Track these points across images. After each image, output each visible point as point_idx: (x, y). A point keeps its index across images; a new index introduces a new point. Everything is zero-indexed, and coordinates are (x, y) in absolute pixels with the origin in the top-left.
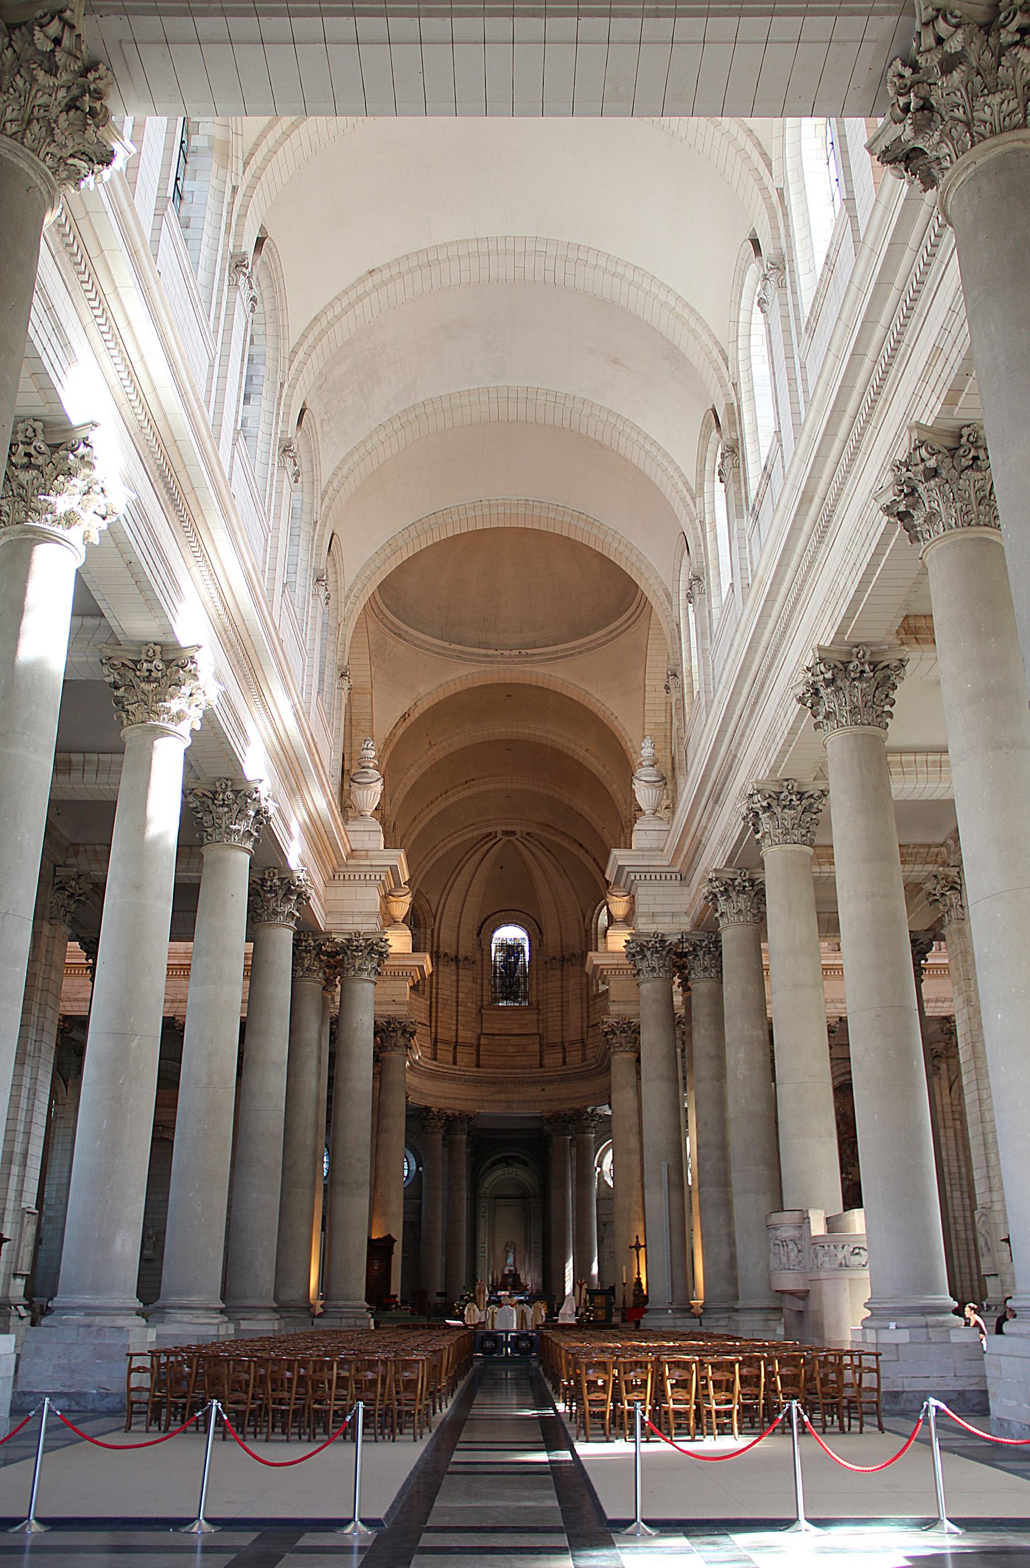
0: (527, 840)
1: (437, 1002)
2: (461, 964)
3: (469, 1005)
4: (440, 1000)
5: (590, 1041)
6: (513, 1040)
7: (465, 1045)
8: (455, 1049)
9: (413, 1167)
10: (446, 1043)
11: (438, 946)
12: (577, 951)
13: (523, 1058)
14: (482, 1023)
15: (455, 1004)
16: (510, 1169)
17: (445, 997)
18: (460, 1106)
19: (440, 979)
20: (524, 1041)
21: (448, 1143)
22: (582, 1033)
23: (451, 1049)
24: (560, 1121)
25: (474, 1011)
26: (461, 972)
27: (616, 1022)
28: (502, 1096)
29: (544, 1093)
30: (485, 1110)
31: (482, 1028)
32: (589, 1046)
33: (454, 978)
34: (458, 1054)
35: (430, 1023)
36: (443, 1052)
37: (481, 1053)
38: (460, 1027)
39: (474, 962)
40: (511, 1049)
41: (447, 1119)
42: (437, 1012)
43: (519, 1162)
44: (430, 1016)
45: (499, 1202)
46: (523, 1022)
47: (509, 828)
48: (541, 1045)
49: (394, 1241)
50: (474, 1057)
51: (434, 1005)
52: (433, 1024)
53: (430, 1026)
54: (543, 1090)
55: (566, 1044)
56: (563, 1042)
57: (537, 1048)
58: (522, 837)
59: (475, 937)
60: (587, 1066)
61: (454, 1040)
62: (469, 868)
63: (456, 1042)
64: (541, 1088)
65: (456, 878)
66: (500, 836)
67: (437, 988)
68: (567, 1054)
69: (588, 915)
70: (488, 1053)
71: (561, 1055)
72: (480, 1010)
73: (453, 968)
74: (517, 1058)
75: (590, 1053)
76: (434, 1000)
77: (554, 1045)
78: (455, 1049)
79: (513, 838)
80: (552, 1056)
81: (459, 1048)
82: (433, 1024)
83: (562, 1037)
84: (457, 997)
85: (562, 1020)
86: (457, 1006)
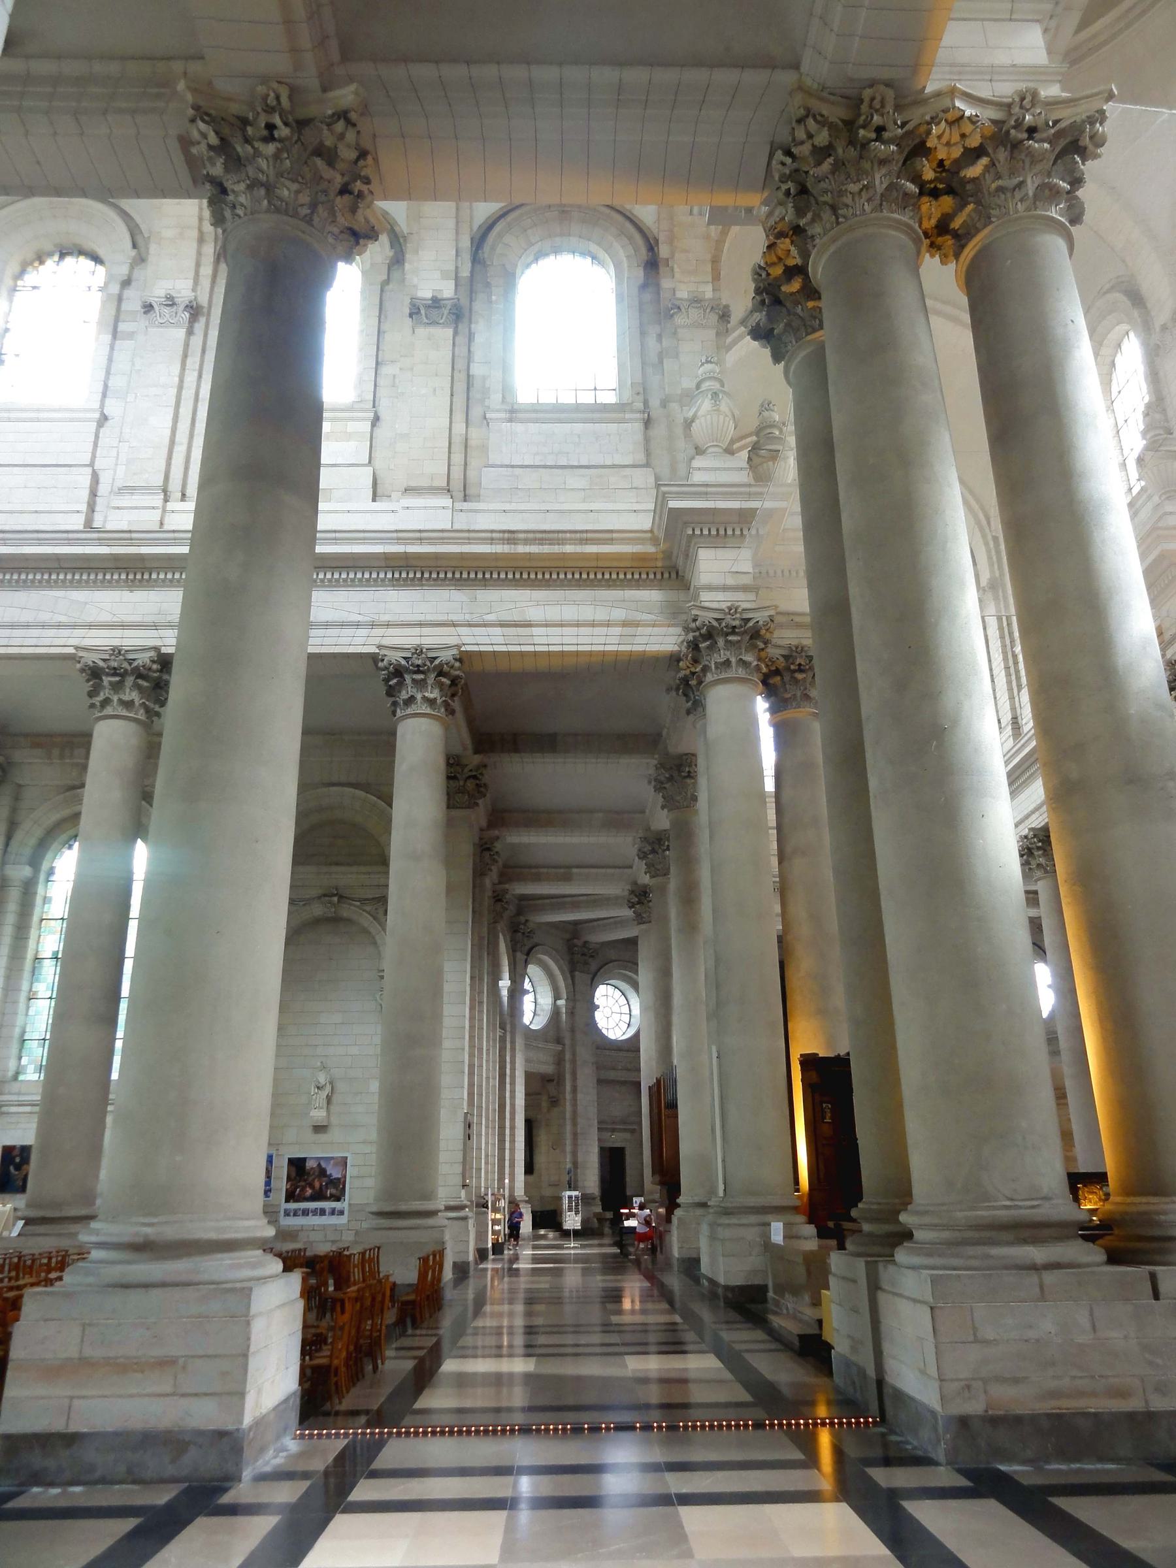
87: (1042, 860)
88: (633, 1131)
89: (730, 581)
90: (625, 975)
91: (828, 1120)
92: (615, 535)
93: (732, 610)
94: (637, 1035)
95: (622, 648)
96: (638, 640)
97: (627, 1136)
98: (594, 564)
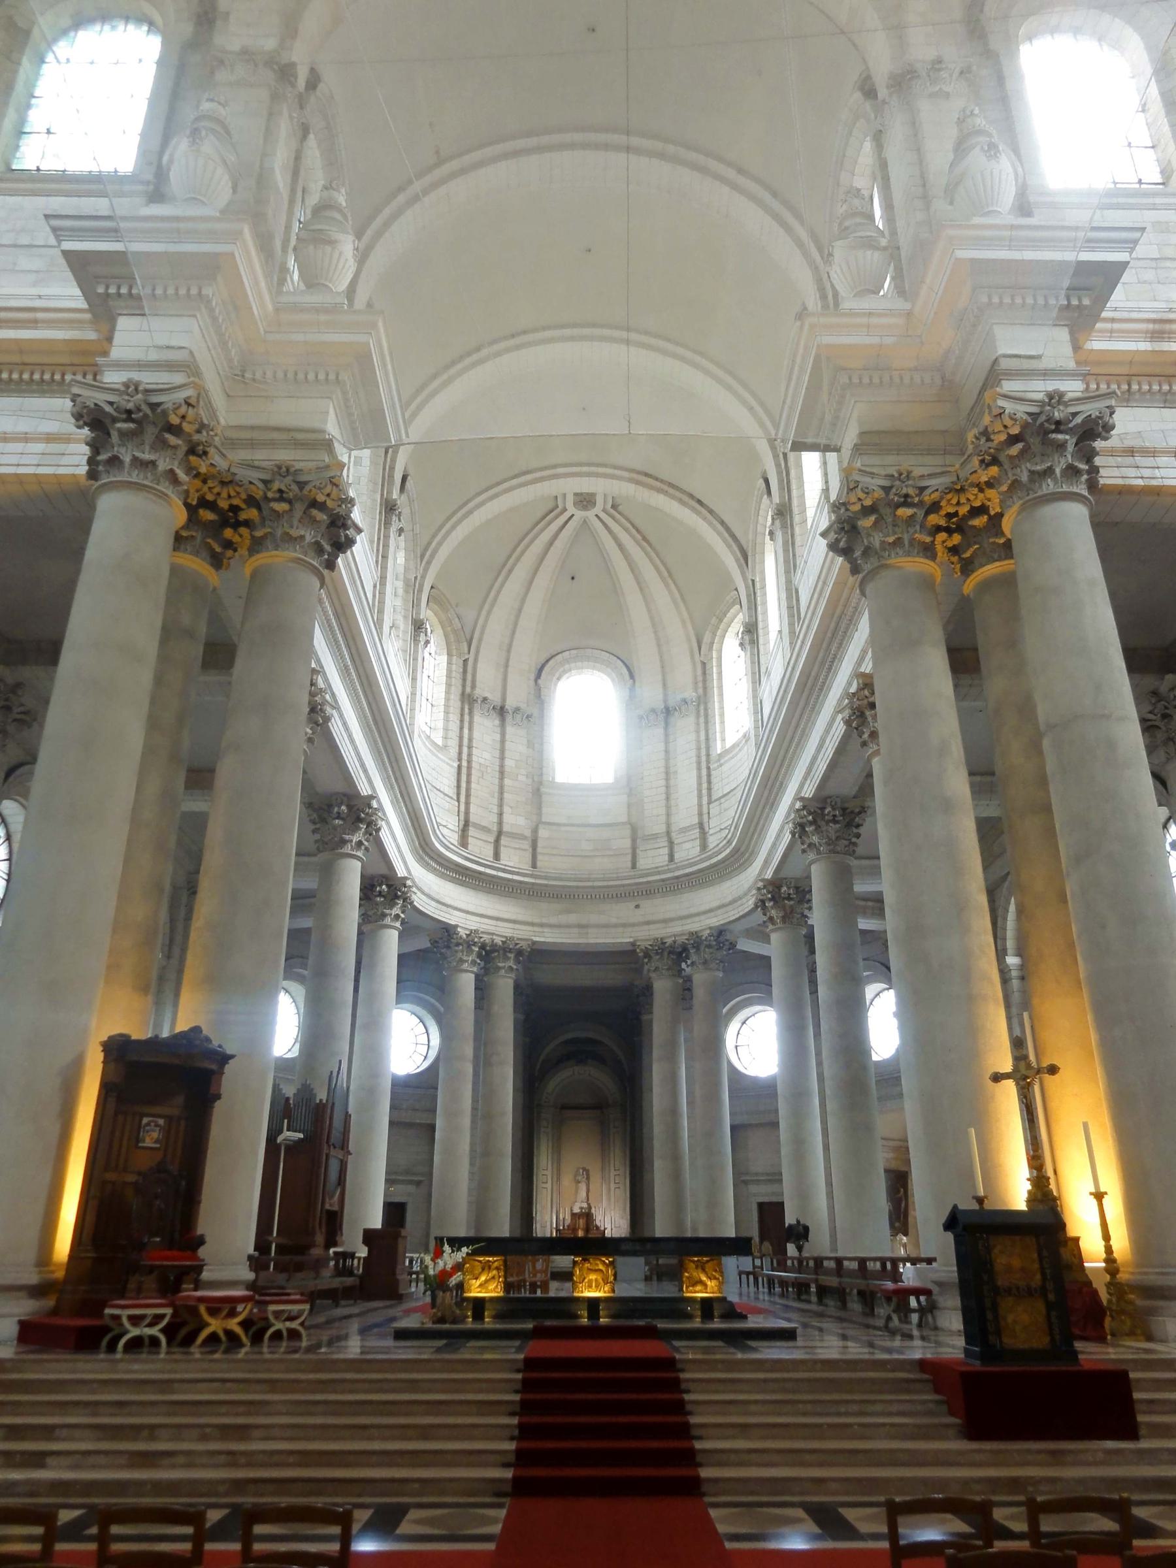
0: (613, 518)
1: (469, 768)
2: (509, 718)
4: (474, 765)
8: (497, 842)
9: (436, 1040)
11: (473, 687)
12: (690, 694)
15: (497, 775)
17: (482, 761)
18: (504, 931)
19: (476, 734)
21: (482, 989)
22: (700, 814)
23: (492, 839)
24: (666, 954)
26: (510, 730)
27: (883, 488)
28: (572, 918)
29: (639, 912)
30: (548, 937)
31: (540, 814)
32: (711, 832)
33: (498, 737)
35: (458, 794)
36: (479, 843)
37: (539, 850)
38: (506, 809)
39: (528, 717)
42: (469, 782)
44: (458, 787)
47: (585, 485)
49: (225, 1059)
50: (528, 856)
51: (464, 771)
53: (458, 800)
54: (637, 906)
55: (673, 835)
56: (668, 833)
57: (627, 843)
58: (604, 510)
59: (532, 683)
61: (495, 828)
62: (521, 572)
65: (502, 585)
66: (571, 509)
67: (470, 747)
69: (706, 639)
71: (666, 851)
73: (497, 722)
75: (713, 841)
76: (464, 764)
77: (655, 837)
78: (497, 842)
79: (590, 514)
80: (650, 853)
83: (668, 825)
84: (502, 766)
85: (668, 799)
86: (502, 778)
87: (815, 839)
88: (418, 1183)
89: (153, 356)
91: (148, 1142)
92: (40, 315)
93: (132, 387)
94: (433, 1070)
95: (41, 470)
96: (65, 460)
97: (411, 1188)
98: (16, 359)
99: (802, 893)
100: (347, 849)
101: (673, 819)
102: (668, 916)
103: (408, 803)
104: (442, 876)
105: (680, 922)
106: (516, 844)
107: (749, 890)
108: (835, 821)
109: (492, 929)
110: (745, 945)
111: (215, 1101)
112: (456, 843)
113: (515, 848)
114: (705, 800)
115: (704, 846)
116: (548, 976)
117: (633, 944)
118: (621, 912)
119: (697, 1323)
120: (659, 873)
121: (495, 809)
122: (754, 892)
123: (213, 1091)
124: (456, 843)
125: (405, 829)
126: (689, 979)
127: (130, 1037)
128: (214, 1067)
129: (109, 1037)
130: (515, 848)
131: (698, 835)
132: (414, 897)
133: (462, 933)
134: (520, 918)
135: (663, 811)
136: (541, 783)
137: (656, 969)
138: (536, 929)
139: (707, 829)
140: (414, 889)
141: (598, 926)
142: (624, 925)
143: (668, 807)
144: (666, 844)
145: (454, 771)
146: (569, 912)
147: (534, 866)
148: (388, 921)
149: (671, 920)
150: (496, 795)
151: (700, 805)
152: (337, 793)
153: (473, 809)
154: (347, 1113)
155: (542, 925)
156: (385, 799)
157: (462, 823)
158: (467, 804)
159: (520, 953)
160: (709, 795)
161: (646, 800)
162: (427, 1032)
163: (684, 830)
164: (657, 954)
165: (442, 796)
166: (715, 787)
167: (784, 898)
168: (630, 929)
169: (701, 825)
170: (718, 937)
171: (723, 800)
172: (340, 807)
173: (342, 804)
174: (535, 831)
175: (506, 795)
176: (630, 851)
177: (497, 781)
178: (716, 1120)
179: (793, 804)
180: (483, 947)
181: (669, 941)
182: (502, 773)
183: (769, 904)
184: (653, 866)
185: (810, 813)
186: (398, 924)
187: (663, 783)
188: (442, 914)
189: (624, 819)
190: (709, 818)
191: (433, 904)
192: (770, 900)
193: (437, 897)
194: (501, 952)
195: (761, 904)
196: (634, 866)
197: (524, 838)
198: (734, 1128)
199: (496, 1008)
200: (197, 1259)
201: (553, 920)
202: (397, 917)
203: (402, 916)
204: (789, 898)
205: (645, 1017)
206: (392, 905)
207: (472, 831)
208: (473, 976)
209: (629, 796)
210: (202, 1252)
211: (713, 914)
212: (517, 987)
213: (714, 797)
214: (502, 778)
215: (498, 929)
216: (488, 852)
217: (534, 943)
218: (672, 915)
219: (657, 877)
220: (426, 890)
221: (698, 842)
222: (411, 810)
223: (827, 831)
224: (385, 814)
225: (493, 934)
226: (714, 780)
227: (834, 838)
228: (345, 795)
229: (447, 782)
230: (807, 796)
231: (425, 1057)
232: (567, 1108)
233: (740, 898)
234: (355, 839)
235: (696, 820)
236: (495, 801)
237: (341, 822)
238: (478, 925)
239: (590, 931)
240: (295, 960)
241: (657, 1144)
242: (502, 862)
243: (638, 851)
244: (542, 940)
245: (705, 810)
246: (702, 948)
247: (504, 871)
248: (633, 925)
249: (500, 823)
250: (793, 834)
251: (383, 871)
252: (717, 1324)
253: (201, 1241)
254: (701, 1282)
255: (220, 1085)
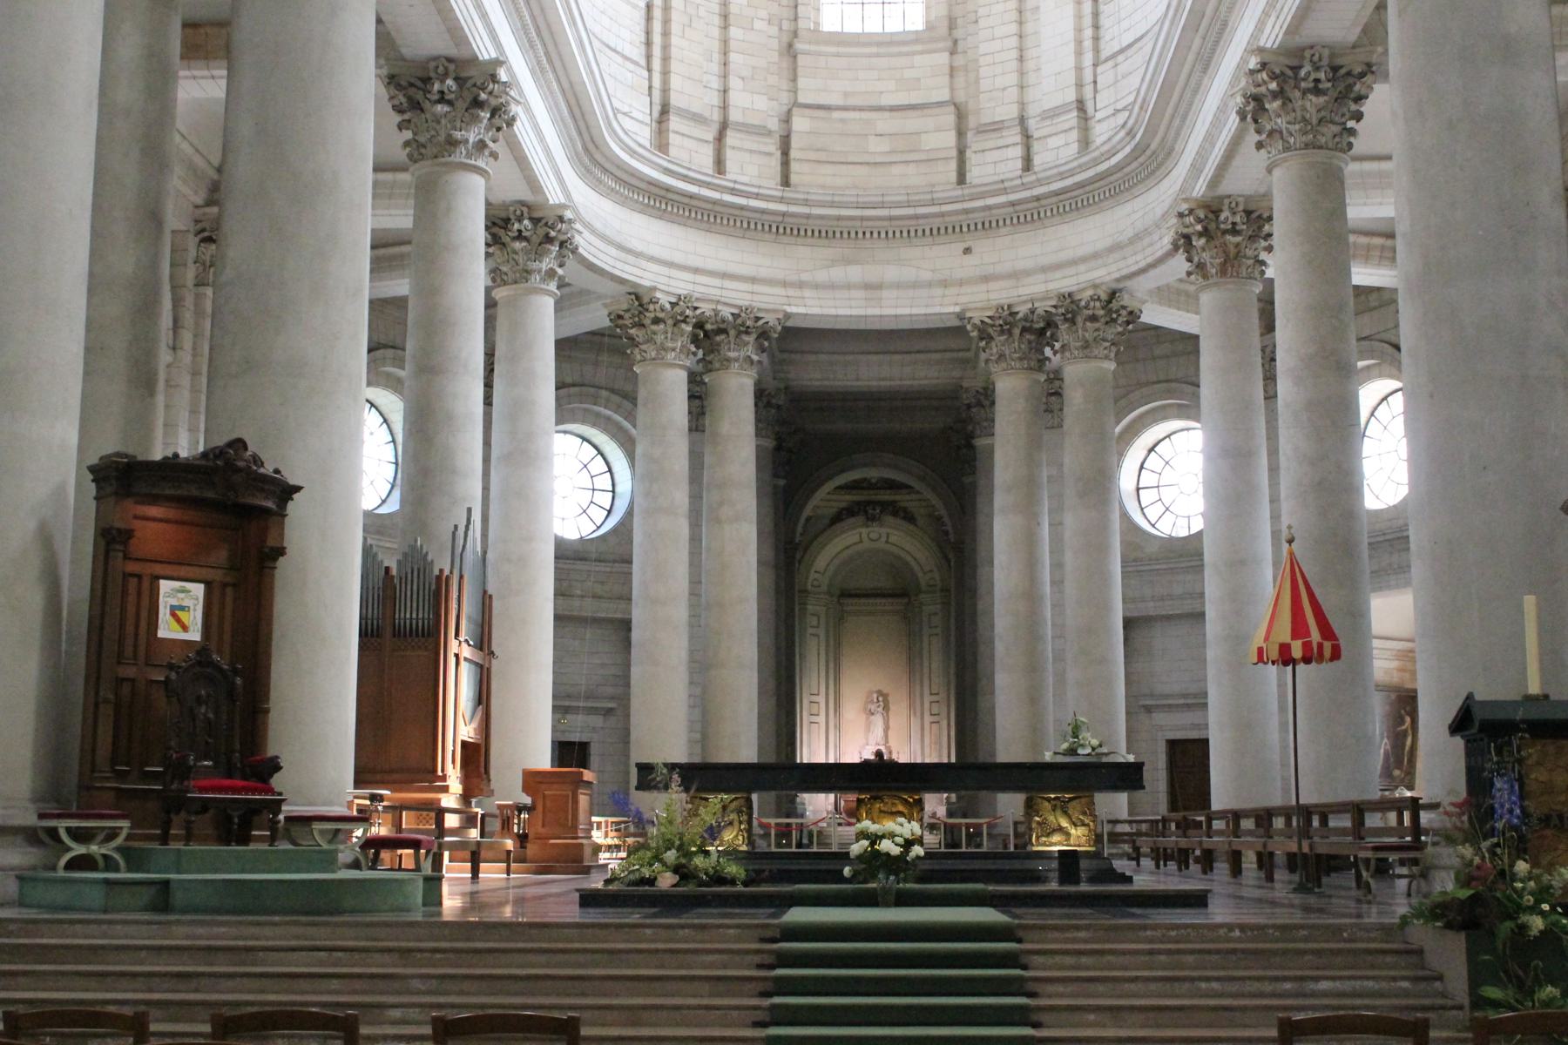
3: (758, 25)
5: (1102, 99)
6: (885, 123)
7: (747, 129)
8: (720, 138)
10: (697, 119)
13: (911, 169)
14: (794, 80)
15: (717, 20)
16: (875, 531)
20: (912, 122)
21: (699, 398)
22: (1079, 85)
23: (710, 134)
24: (1017, 331)
25: (775, 44)
28: (854, 273)
29: (969, 260)
31: (795, 91)
32: (1099, 115)
34: (731, 158)
35: (649, 57)
37: (793, 154)
38: (734, 83)
40: (877, 147)
41: (700, 325)
42: (666, 34)
43: (895, 514)
44: (648, 43)
45: (852, 604)
46: (908, 74)
48: (961, 134)
49: (287, 492)
50: (775, 161)
52: (657, 64)
53: (649, 70)
54: (967, 251)
55: (1032, 124)
56: (1022, 120)
57: (950, 139)
60: (1096, 161)
61: (716, 116)
63: (724, 127)
64: (963, 246)
68: (1036, 147)
70: (812, 156)
71: (1018, 152)
72: (790, 46)
74: (896, 170)
75: (1102, 132)
77: (996, 127)
78: (720, 138)
81: (732, 138)
82: (657, 64)
83: (1022, 105)
85: (1021, 59)
86: (725, 27)
90: (598, 415)
94: (623, 531)
97: (597, 721)
99: (1256, 220)
100: (460, 156)
101: (1031, 95)
102: (1021, 265)
103: (561, 73)
104: (623, 202)
105: (1042, 277)
106: (750, 142)
107: (1164, 216)
108: (1317, 91)
109: (715, 293)
110: (1155, 315)
111: (275, 559)
112: (647, 145)
113: (751, 151)
114: (1088, 59)
115: (1085, 142)
116: (815, 374)
117: (960, 316)
118: (943, 258)
119: (1053, 886)
120: (1005, 191)
121: (715, 83)
122: (1174, 220)
123: (271, 542)
124: (648, 145)
125: (558, 121)
126: (1056, 376)
127: (135, 457)
128: (270, 504)
129: (101, 459)
130: (751, 151)
131: (1074, 122)
132: (578, 239)
133: (665, 300)
134: (764, 273)
135: (1012, 79)
136: (795, 34)
137: (1001, 357)
138: (791, 292)
139: (1090, 110)
140: (578, 226)
141: (898, 286)
142: (944, 284)
143: (1022, 73)
144: (1018, 139)
145: (639, 15)
146: (848, 262)
147: (786, 182)
148: (535, 279)
149: (1027, 273)
150: (716, 57)
151: (1079, 69)
152: (436, 58)
153: (675, 82)
154: (485, 592)
155: (801, 285)
156: (519, 69)
157: (657, 109)
158: (666, 73)
159: (764, 334)
160: (1096, 50)
161: (982, 61)
162: (610, 470)
163: (1051, 114)
164: (1002, 332)
165: (619, 59)
166: (1106, 35)
167: (1225, 232)
168: (952, 291)
169: (1081, 105)
170: (1110, 302)
171: (1120, 58)
172: (442, 82)
173: (446, 75)
174: (787, 120)
175: (733, 57)
176: (954, 153)
177: (716, 32)
178: (1104, 607)
179: (1244, 60)
180: (700, 325)
181: (1022, 310)
182: (725, 17)
183: (1199, 242)
184: (996, 178)
185: (1274, 76)
186: (553, 286)
187: (1014, 28)
188: (627, 268)
189: (944, 95)
190: (1096, 91)
191: (613, 251)
192: (1200, 235)
193: (618, 239)
194: (732, 333)
195: (1184, 242)
196: (961, 179)
197: (769, 133)
198: (1128, 623)
199: (725, 428)
200: (271, 791)
201: (822, 276)
202: (551, 274)
203: (560, 271)
204: (1234, 231)
205: (980, 442)
206: (539, 255)
207: (675, 122)
208: (683, 375)
209: (953, 53)
210: (277, 781)
211: (1100, 261)
212: (760, 394)
213: (1104, 54)
214: (725, 27)
215: (725, 293)
216: (703, 159)
217: (788, 316)
218: (1029, 264)
219: (1002, 199)
220: (598, 225)
221: (1074, 135)
222: (566, 85)
223: (1304, 109)
224: (521, 93)
225: (718, 302)
226: (1105, 22)
227: (1314, 121)
228: (450, 60)
229: (629, 37)
230: (1269, 45)
231: (609, 512)
232: (846, 595)
233: (1146, 232)
234: (472, 137)
235: (1071, 96)
236: (715, 67)
237: (446, 108)
238: (691, 287)
239: (885, 293)
240: (381, 351)
241: (999, 647)
242: (728, 176)
243: (969, 153)
244: (801, 310)
245: (1088, 76)
246: (1079, 320)
247: (733, 192)
248: (961, 283)
249: (725, 107)
250: (1242, 115)
251: (525, 194)
252: (1084, 887)
253: (274, 766)
254: (1060, 829)
255: (282, 535)
